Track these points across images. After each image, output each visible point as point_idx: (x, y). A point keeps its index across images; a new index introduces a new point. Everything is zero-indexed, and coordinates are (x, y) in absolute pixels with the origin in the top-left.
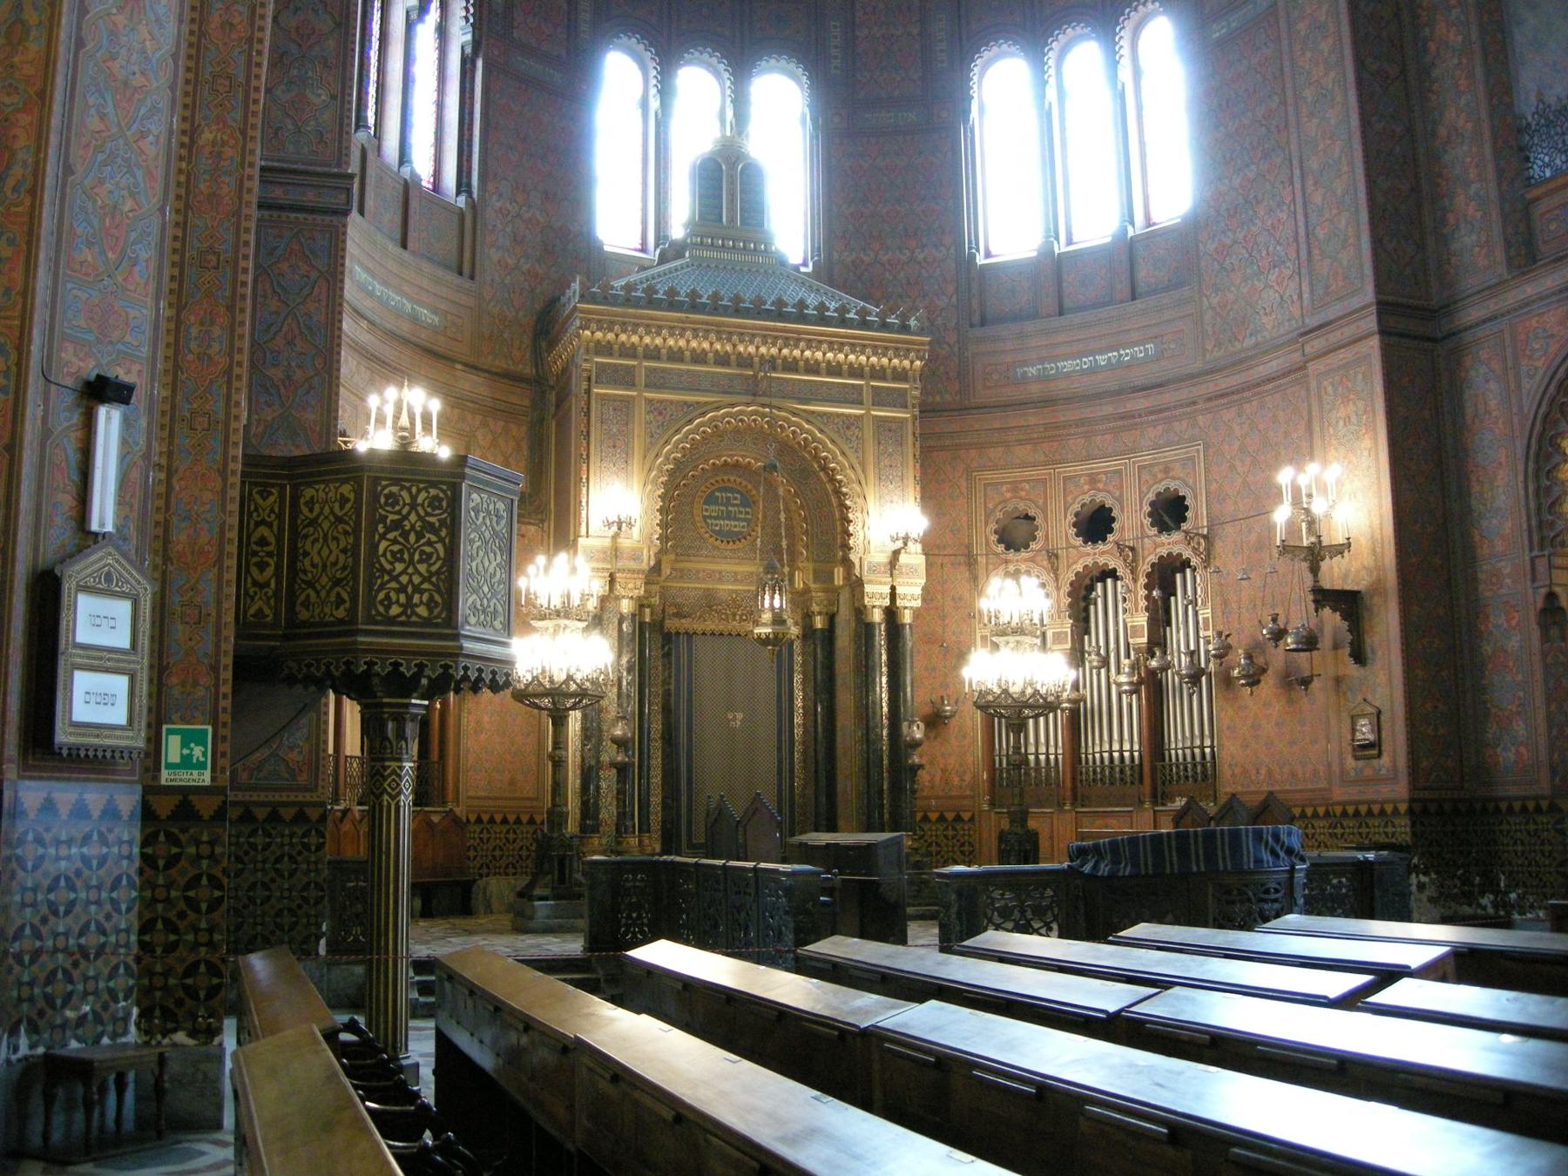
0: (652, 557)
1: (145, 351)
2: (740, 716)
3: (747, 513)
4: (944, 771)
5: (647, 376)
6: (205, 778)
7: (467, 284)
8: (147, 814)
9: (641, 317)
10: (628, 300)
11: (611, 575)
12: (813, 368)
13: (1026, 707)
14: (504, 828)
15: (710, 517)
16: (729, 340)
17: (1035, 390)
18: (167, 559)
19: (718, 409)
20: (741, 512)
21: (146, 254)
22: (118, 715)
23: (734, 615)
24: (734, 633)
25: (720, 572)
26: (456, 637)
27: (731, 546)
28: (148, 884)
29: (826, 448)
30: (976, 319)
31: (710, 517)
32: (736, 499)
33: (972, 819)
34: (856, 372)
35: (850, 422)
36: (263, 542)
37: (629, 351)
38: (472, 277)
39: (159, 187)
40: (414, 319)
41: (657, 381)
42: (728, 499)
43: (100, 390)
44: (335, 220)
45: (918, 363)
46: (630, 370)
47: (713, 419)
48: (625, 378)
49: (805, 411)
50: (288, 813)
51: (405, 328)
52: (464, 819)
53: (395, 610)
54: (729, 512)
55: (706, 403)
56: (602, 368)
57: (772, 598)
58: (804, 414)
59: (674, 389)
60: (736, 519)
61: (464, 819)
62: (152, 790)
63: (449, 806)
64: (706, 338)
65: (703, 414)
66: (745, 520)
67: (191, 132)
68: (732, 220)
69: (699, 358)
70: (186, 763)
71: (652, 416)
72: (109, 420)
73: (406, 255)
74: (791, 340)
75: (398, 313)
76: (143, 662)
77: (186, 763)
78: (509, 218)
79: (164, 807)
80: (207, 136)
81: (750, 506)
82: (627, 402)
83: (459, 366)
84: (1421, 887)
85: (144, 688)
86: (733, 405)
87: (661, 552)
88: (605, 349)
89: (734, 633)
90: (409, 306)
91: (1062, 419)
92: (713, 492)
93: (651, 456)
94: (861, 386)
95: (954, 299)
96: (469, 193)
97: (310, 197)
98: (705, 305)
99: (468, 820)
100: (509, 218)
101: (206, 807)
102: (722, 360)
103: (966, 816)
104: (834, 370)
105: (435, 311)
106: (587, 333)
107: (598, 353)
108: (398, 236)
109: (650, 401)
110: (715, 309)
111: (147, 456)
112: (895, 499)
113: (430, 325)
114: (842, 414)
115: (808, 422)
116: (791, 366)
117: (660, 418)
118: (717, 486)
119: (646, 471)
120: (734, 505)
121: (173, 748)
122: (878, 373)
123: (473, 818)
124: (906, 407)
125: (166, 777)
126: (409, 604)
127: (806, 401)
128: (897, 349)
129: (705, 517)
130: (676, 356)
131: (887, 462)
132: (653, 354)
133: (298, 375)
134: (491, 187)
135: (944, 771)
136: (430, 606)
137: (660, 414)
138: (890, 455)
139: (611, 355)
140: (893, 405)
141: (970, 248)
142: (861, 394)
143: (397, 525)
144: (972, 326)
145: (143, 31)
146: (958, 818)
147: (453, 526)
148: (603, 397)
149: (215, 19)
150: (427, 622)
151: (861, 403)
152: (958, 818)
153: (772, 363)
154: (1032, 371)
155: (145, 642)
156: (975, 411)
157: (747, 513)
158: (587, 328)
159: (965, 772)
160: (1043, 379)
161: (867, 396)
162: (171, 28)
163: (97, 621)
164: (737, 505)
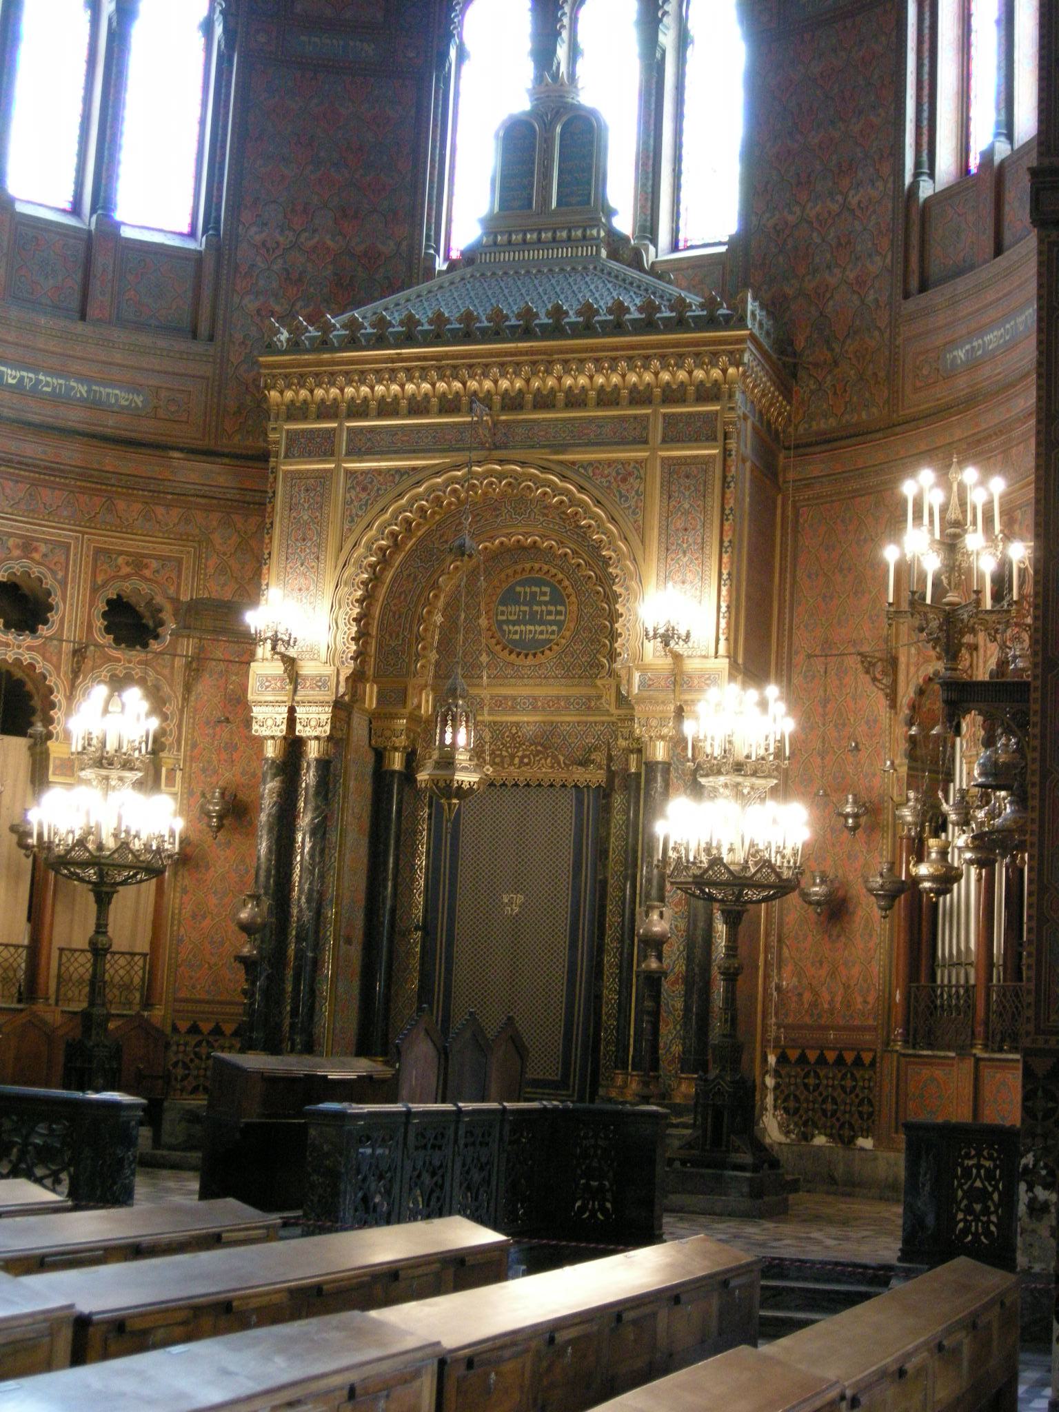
0: (342, 683)
2: (520, 898)
3: (559, 613)
4: (847, 987)
5: (349, 441)
7: (198, 347)
9: (307, 364)
10: (324, 342)
11: (292, 711)
12: (575, 400)
13: (750, 886)
14: (193, 1040)
15: (508, 622)
16: (456, 378)
17: (961, 384)
19: (438, 474)
20: (550, 613)
23: (512, 757)
24: (546, 783)
25: (514, 698)
27: (530, 661)
29: (588, 513)
30: (914, 283)
31: (508, 622)
32: (544, 594)
33: (873, 1063)
34: (640, 397)
35: (627, 472)
37: (327, 411)
38: (211, 338)
40: (94, 404)
41: (363, 445)
42: (533, 594)
45: (731, 370)
46: (330, 435)
47: (432, 489)
48: (323, 446)
49: (561, 463)
51: (74, 417)
52: (168, 1030)
54: (533, 614)
55: (425, 468)
56: (293, 437)
57: (443, 732)
58: (558, 468)
59: (382, 453)
60: (542, 622)
61: (168, 1030)
63: (40, 1007)
64: (424, 378)
65: (418, 483)
66: (551, 623)
68: (546, 200)
69: (417, 407)
71: (353, 494)
73: (80, 327)
74: (545, 362)
75: (56, 398)
78: (278, 253)
81: (563, 603)
82: (323, 476)
83: (176, 454)
84: (1038, 1210)
86: (457, 467)
87: (357, 678)
88: (296, 412)
89: (546, 783)
90: (83, 389)
91: (984, 426)
92: (512, 588)
93: (348, 546)
94: (647, 416)
95: (888, 260)
96: (217, 229)
98: (484, 331)
99: (175, 1029)
100: (278, 253)
102: (449, 405)
103: (867, 1058)
104: (607, 398)
105: (135, 388)
106: (274, 395)
107: (290, 418)
108: (75, 304)
109: (350, 473)
110: (497, 333)
112: (689, 576)
113: (123, 407)
114: (616, 461)
115: (563, 477)
116: (544, 401)
117: (363, 495)
118: (518, 578)
119: (339, 568)
120: (540, 603)
122: (672, 395)
123: (184, 1026)
124: (715, 439)
127: (564, 448)
128: (697, 355)
129: (500, 623)
130: (387, 408)
131: (680, 524)
132: (359, 410)
134: (246, 216)
135: (847, 987)
137: (364, 489)
138: (687, 513)
139: (305, 418)
140: (696, 438)
141: (917, 174)
142: (646, 428)
144: (907, 295)
146: (858, 1062)
148: (286, 473)
151: (646, 442)
152: (858, 1062)
153: (513, 402)
154: (961, 354)
156: (898, 429)
157: (559, 613)
158: (274, 387)
159: (868, 990)
160: (973, 364)
161: (657, 431)
164: (546, 603)
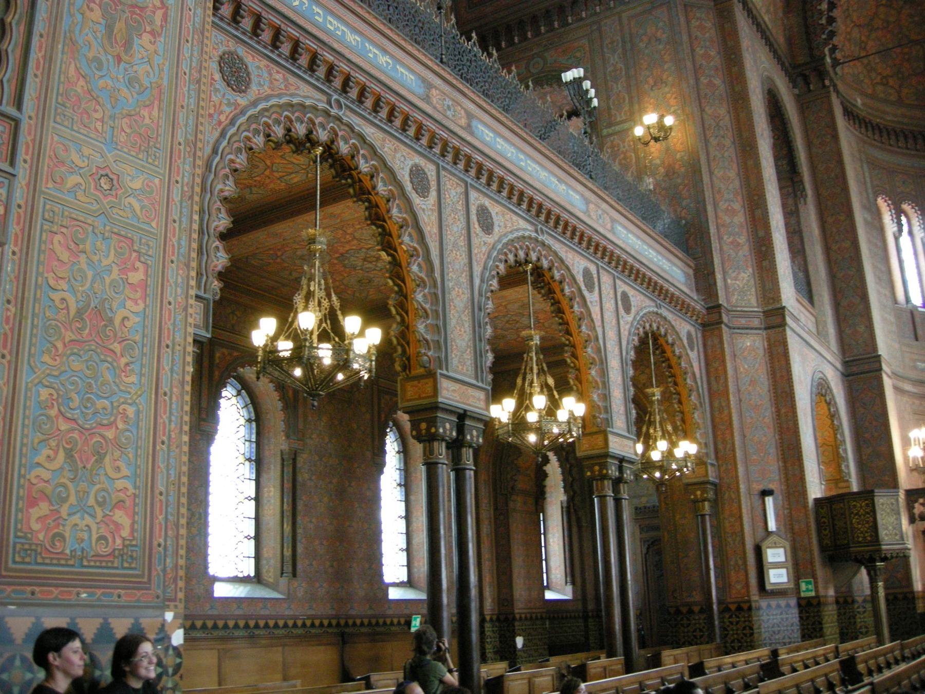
1: (777, 478)
6: (813, 594)
8: (799, 605)
18: (794, 534)
21: (773, 450)
22: (784, 579)
26: (880, 545)
28: (802, 625)
36: (824, 523)
39: (772, 430)
43: (765, 493)
44: (878, 373)
50: (900, 596)
53: (861, 539)
62: (800, 599)
67: (778, 411)
70: (808, 590)
72: (769, 501)
76: (790, 565)
77: (808, 590)
79: (803, 603)
80: (783, 411)
85: (791, 570)
97: (866, 367)
101: (815, 602)
111: (783, 506)
121: (803, 586)
125: (803, 595)
126: (865, 538)
133: (876, 434)
136: (871, 536)
143: (857, 514)
145: (758, 389)
147: (874, 511)
149: (778, 375)
150: (871, 541)
155: (789, 558)
162: (766, 383)
163: (774, 555)
